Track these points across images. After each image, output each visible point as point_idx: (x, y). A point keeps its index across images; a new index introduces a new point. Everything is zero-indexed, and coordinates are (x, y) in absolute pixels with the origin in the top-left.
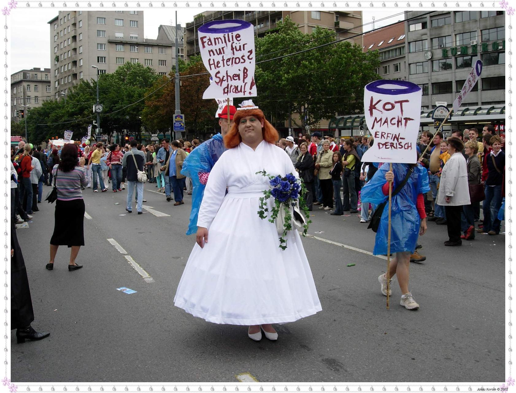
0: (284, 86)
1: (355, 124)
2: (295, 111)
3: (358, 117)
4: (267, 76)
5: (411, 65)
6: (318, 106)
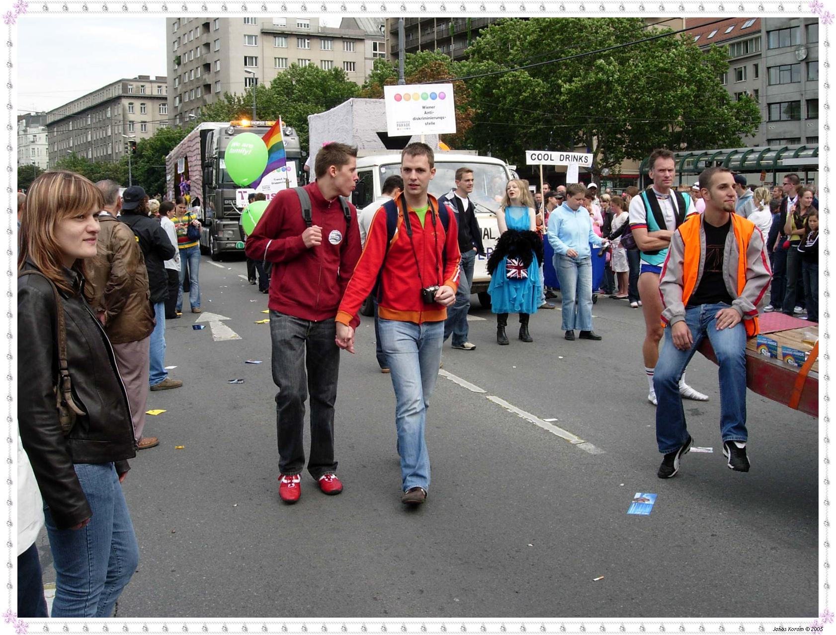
0: (565, 102)
1: (686, 167)
2: (580, 145)
3: (692, 155)
4: (539, 84)
5: (772, 70)
6: (619, 136)
